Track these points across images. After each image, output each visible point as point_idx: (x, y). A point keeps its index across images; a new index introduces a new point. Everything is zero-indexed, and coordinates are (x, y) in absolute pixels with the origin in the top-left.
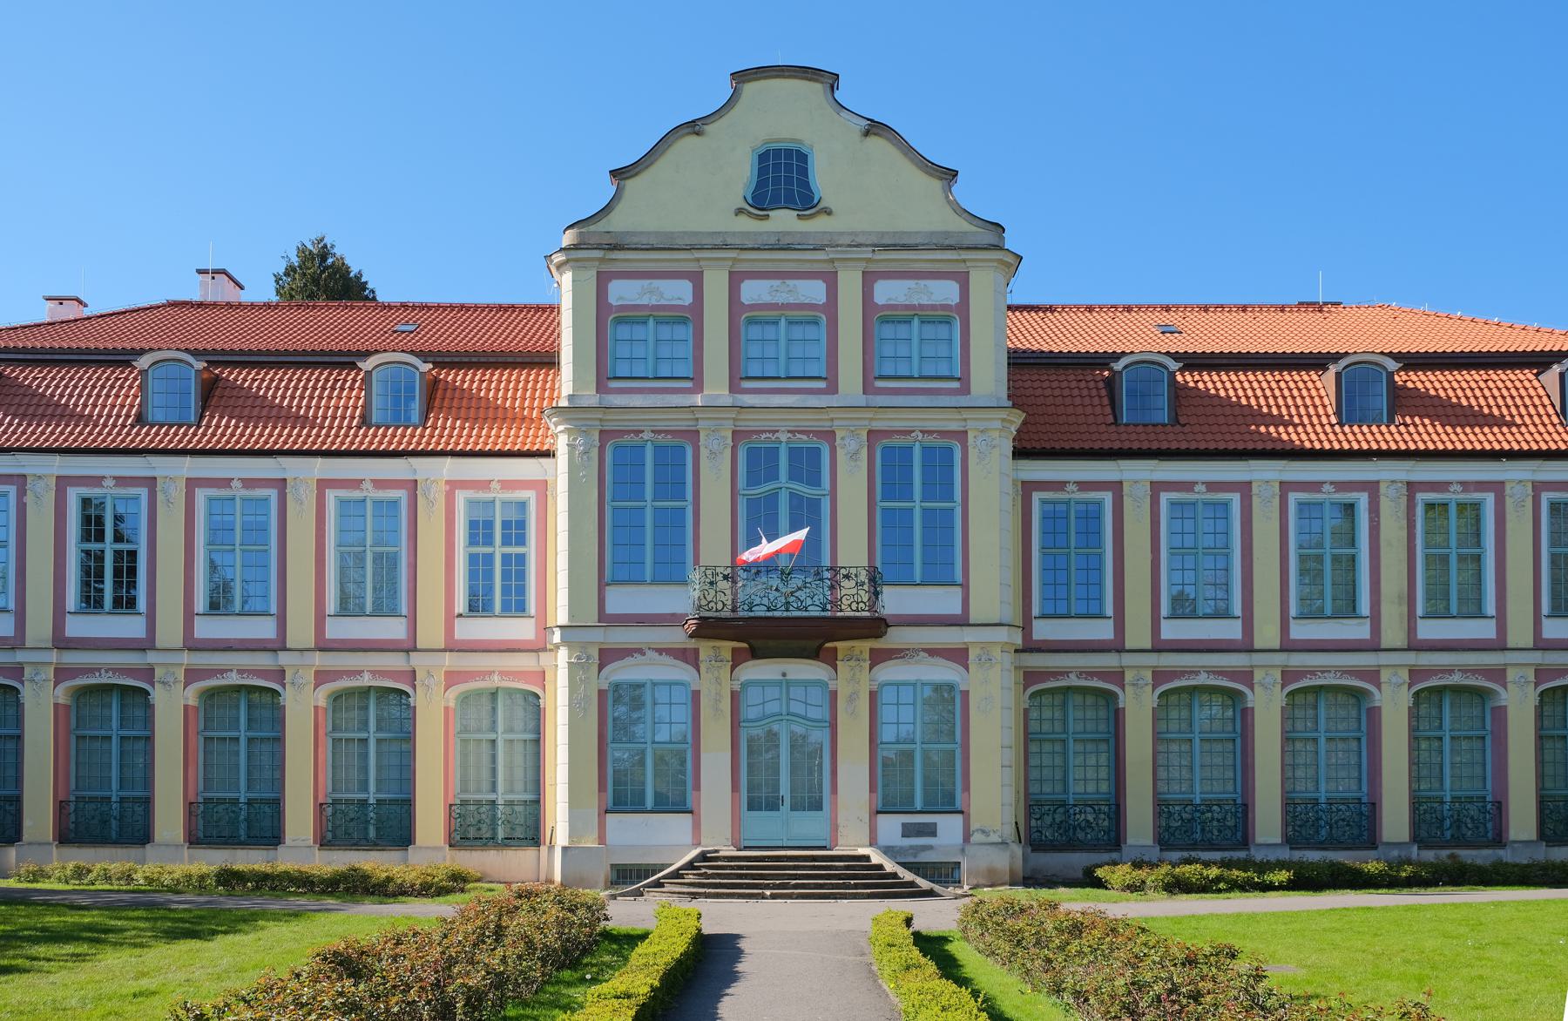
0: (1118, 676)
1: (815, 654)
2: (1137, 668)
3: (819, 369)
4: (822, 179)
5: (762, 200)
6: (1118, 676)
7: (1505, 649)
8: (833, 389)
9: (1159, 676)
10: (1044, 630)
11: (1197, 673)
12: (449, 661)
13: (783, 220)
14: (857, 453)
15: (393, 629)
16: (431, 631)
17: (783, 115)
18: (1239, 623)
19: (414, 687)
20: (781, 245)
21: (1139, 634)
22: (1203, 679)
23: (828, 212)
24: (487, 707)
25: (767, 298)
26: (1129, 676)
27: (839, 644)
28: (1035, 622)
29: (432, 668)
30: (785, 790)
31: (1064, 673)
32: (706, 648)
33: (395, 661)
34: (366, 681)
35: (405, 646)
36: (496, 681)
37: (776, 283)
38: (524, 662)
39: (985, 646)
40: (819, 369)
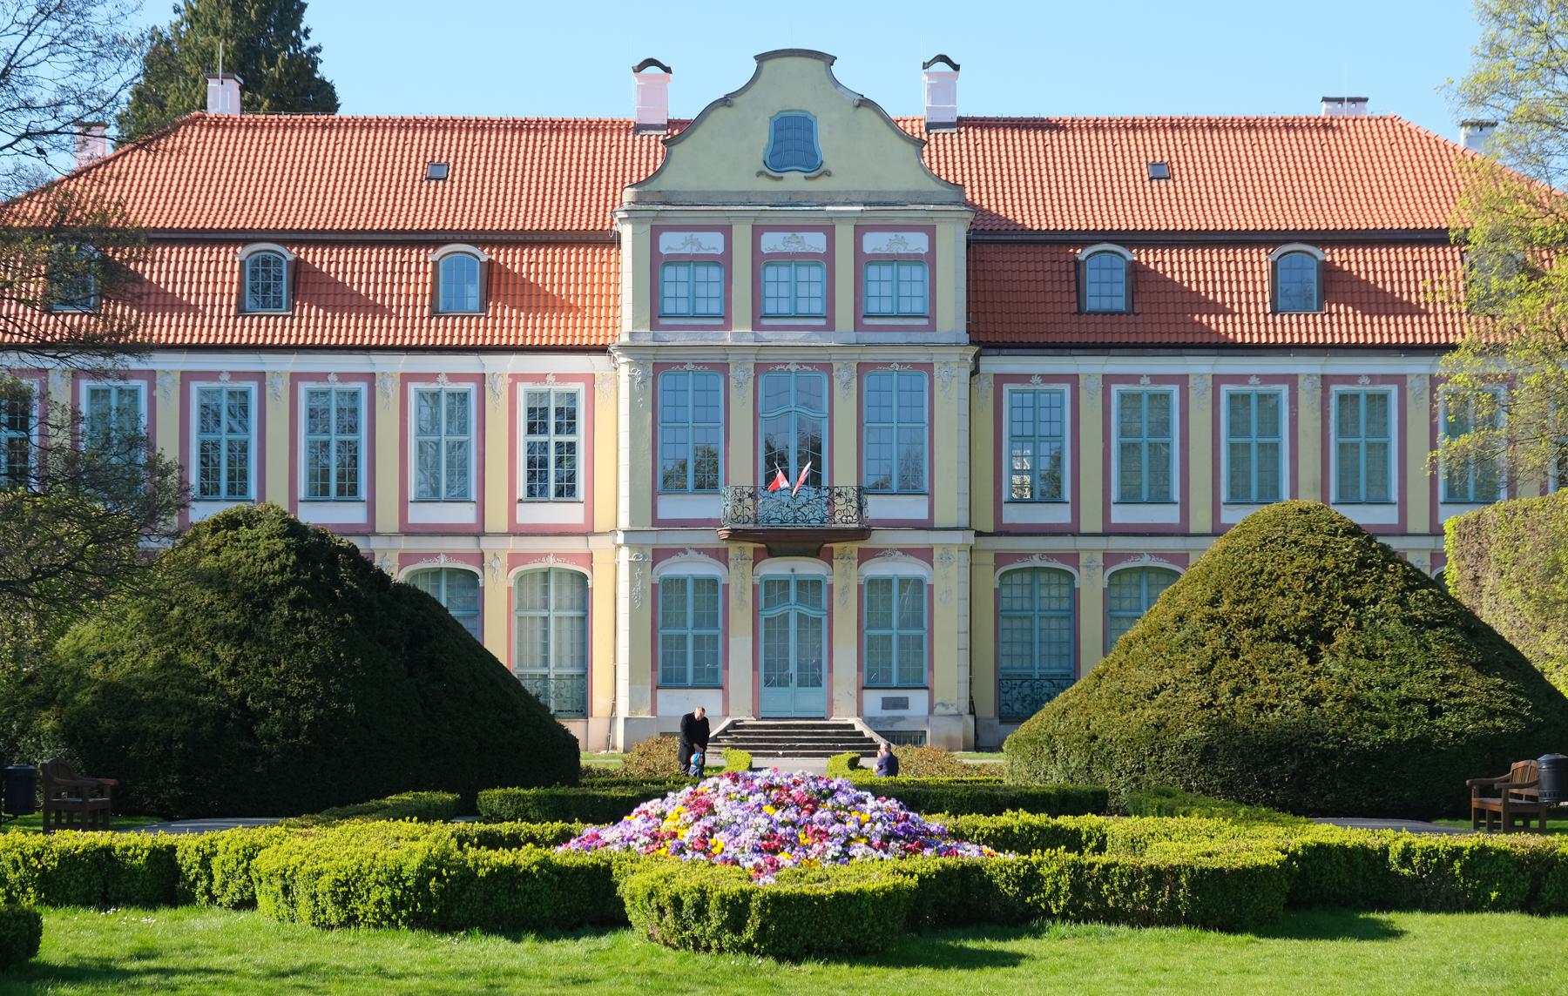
0: (1073, 558)
1: (816, 554)
2: (1091, 550)
3: (817, 307)
4: (826, 142)
5: (777, 163)
6: (1073, 558)
7: (1405, 534)
8: (830, 327)
9: (1110, 559)
10: (1012, 515)
11: (1141, 555)
12: (514, 544)
13: (794, 181)
14: (848, 382)
15: (463, 514)
16: (496, 519)
17: (794, 91)
18: (1177, 508)
19: (483, 569)
20: (793, 200)
21: (1091, 520)
22: (1146, 561)
23: (828, 174)
24: (539, 578)
25: (781, 248)
26: (1083, 559)
27: (834, 545)
28: (1005, 507)
29: (498, 549)
30: (793, 669)
31: (1029, 555)
32: (734, 549)
33: (466, 545)
34: (442, 562)
35: (475, 530)
36: (551, 562)
37: (789, 235)
38: (575, 545)
39: (945, 547)
40: (817, 307)
